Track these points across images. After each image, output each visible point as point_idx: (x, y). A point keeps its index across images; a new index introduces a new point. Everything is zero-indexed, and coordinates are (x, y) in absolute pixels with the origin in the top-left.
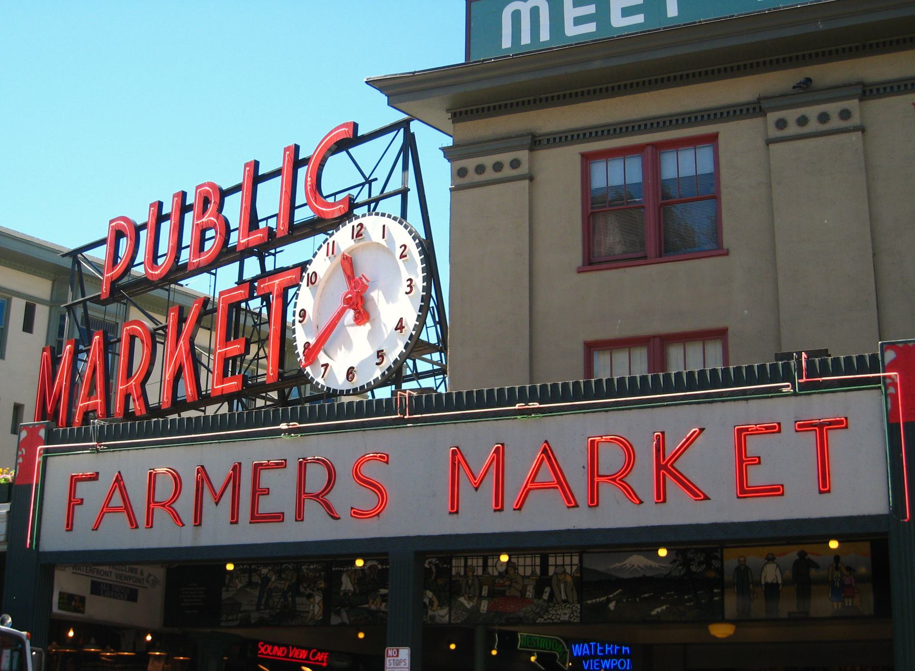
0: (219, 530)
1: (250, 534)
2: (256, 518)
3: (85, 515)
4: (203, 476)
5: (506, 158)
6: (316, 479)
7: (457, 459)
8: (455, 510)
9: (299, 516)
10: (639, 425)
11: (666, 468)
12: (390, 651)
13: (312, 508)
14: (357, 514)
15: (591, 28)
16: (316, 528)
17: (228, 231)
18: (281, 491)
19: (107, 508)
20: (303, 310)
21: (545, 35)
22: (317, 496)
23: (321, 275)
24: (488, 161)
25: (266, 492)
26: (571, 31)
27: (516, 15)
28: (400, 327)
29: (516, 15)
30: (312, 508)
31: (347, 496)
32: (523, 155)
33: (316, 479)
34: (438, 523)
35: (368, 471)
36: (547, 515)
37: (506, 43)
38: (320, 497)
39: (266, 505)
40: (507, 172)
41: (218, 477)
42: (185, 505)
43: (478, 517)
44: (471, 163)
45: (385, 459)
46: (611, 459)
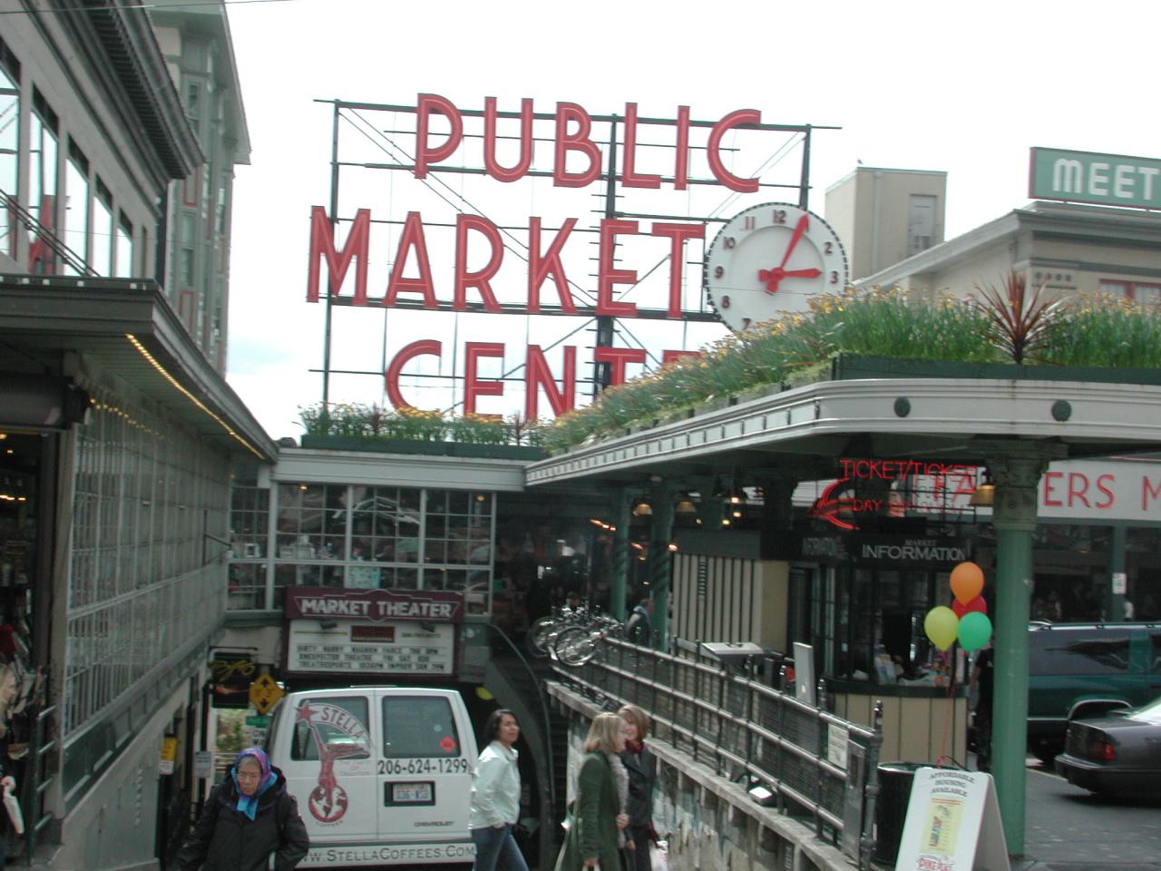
2: (1048, 503)
5: (1064, 272)
6: (1078, 485)
7: (1146, 483)
8: (1145, 507)
9: (1070, 504)
12: (1115, 575)
13: (1076, 500)
14: (1098, 505)
15: (1103, 192)
16: (1078, 512)
17: (595, 155)
20: (720, 268)
21: (1078, 190)
22: (1080, 495)
23: (738, 240)
24: (1054, 271)
25: (1051, 489)
26: (1094, 191)
27: (1063, 168)
29: (1063, 168)
30: (1076, 500)
31: (1094, 495)
32: (1071, 272)
35: (1105, 483)
37: (1056, 187)
38: (1080, 495)
39: (1053, 497)
40: (1063, 282)
44: (1044, 271)
45: (1111, 477)
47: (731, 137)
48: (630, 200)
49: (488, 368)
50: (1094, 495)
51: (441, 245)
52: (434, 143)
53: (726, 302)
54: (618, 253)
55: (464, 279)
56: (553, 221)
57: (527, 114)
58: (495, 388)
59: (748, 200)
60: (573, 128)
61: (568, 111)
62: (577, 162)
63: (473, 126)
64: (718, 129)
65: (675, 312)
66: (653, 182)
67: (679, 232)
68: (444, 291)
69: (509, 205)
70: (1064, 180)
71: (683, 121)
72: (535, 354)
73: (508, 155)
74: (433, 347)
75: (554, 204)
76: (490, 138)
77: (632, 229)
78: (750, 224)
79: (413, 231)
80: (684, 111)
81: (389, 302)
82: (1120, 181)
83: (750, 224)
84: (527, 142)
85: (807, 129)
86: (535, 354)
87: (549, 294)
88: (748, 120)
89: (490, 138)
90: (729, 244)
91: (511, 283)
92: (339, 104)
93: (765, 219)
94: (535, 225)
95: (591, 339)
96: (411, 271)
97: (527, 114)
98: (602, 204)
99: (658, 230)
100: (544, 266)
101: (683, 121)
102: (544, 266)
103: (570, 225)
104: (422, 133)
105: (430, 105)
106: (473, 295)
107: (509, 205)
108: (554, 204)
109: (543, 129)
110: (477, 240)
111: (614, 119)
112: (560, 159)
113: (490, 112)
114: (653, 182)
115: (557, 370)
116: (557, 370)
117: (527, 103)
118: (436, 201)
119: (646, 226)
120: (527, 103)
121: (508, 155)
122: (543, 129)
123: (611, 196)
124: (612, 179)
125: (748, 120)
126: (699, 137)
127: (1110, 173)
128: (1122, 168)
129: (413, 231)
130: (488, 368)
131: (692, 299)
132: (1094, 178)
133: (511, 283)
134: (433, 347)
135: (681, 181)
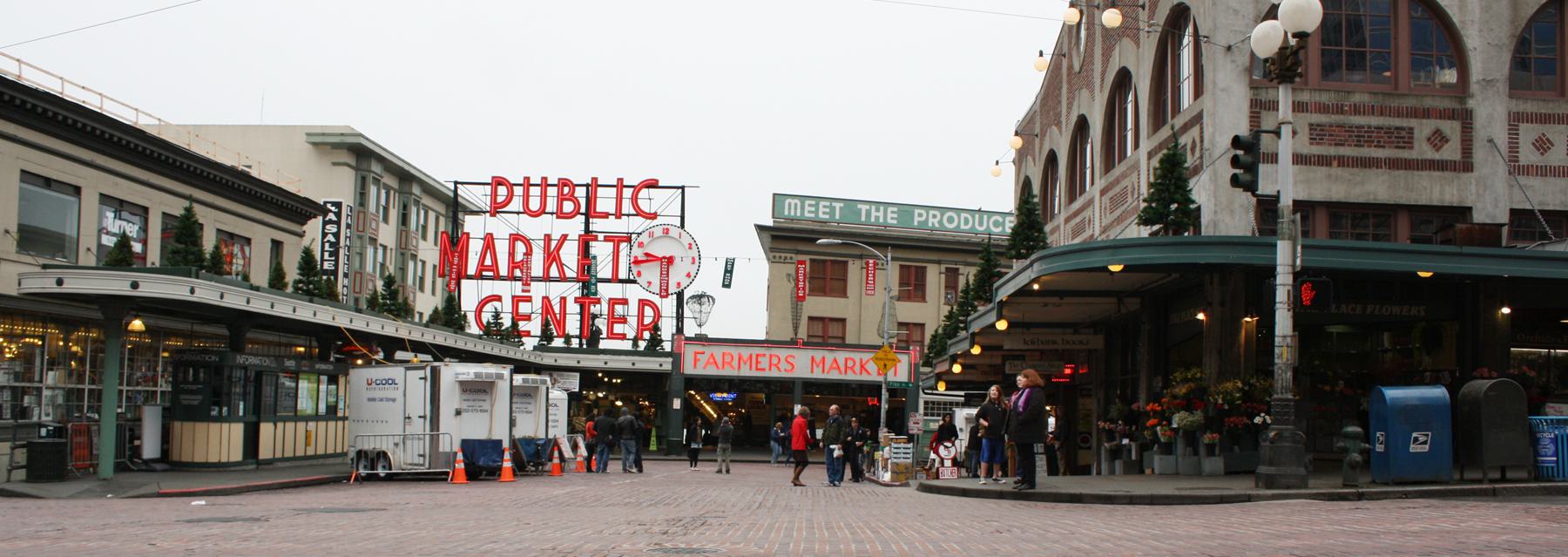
0: (746, 372)
1: (754, 373)
3: (700, 364)
4: (740, 357)
10: (857, 356)
11: (862, 367)
16: (774, 373)
18: (764, 363)
19: (708, 363)
26: (807, 215)
28: (688, 275)
31: (783, 365)
33: (775, 361)
34: (806, 374)
36: (834, 375)
41: (745, 356)
42: (735, 363)
43: (818, 374)
46: (850, 363)
47: (644, 193)
48: (597, 225)
49: (524, 308)
50: (783, 365)
51: (502, 248)
52: (500, 199)
53: (639, 274)
54: (593, 251)
55: (513, 264)
56: (556, 236)
57: (544, 184)
58: (528, 318)
59: (655, 222)
60: (566, 190)
61: (564, 183)
62: (568, 207)
63: (518, 191)
64: (637, 189)
65: (615, 279)
66: (606, 215)
67: (616, 240)
68: (503, 271)
69: (535, 229)
70: (791, 210)
71: (620, 185)
72: (546, 299)
73: (535, 204)
74: (499, 298)
75: (557, 227)
76: (526, 197)
77: (596, 239)
78: (651, 235)
79: (489, 242)
80: (620, 180)
81: (479, 276)
82: (821, 209)
83: (651, 235)
84: (544, 197)
85: (683, 188)
86: (546, 299)
87: (554, 272)
88: (652, 184)
89: (526, 197)
90: (641, 245)
91: (537, 269)
92: (456, 183)
93: (658, 232)
94: (548, 238)
95: (578, 294)
96: (488, 262)
97: (544, 184)
98: (583, 227)
99: (607, 239)
100: (552, 256)
101: (620, 185)
102: (552, 256)
103: (564, 237)
104: (494, 194)
105: (498, 182)
106: (518, 273)
107: (535, 229)
108: (557, 227)
109: (552, 191)
110: (520, 248)
111: (587, 186)
112: (560, 206)
113: (527, 184)
114: (606, 215)
115: (557, 310)
116: (557, 310)
117: (545, 179)
118: (501, 227)
119: (601, 237)
120: (545, 179)
121: (535, 204)
122: (552, 191)
123: (587, 224)
124: (588, 216)
125: (652, 184)
126: (627, 193)
127: (817, 206)
128: (822, 203)
129: (489, 242)
130: (524, 308)
131: (623, 275)
132: (807, 208)
133: (537, 269)
134: (499, 298)
135: (619, 215)
